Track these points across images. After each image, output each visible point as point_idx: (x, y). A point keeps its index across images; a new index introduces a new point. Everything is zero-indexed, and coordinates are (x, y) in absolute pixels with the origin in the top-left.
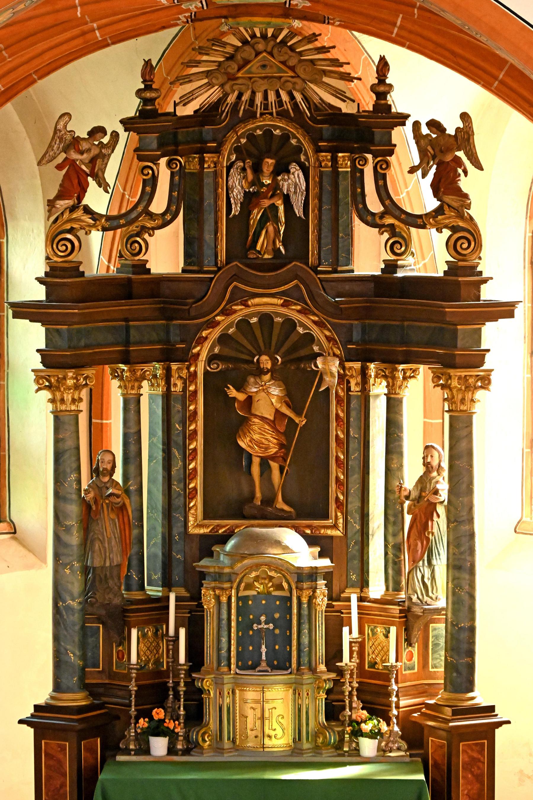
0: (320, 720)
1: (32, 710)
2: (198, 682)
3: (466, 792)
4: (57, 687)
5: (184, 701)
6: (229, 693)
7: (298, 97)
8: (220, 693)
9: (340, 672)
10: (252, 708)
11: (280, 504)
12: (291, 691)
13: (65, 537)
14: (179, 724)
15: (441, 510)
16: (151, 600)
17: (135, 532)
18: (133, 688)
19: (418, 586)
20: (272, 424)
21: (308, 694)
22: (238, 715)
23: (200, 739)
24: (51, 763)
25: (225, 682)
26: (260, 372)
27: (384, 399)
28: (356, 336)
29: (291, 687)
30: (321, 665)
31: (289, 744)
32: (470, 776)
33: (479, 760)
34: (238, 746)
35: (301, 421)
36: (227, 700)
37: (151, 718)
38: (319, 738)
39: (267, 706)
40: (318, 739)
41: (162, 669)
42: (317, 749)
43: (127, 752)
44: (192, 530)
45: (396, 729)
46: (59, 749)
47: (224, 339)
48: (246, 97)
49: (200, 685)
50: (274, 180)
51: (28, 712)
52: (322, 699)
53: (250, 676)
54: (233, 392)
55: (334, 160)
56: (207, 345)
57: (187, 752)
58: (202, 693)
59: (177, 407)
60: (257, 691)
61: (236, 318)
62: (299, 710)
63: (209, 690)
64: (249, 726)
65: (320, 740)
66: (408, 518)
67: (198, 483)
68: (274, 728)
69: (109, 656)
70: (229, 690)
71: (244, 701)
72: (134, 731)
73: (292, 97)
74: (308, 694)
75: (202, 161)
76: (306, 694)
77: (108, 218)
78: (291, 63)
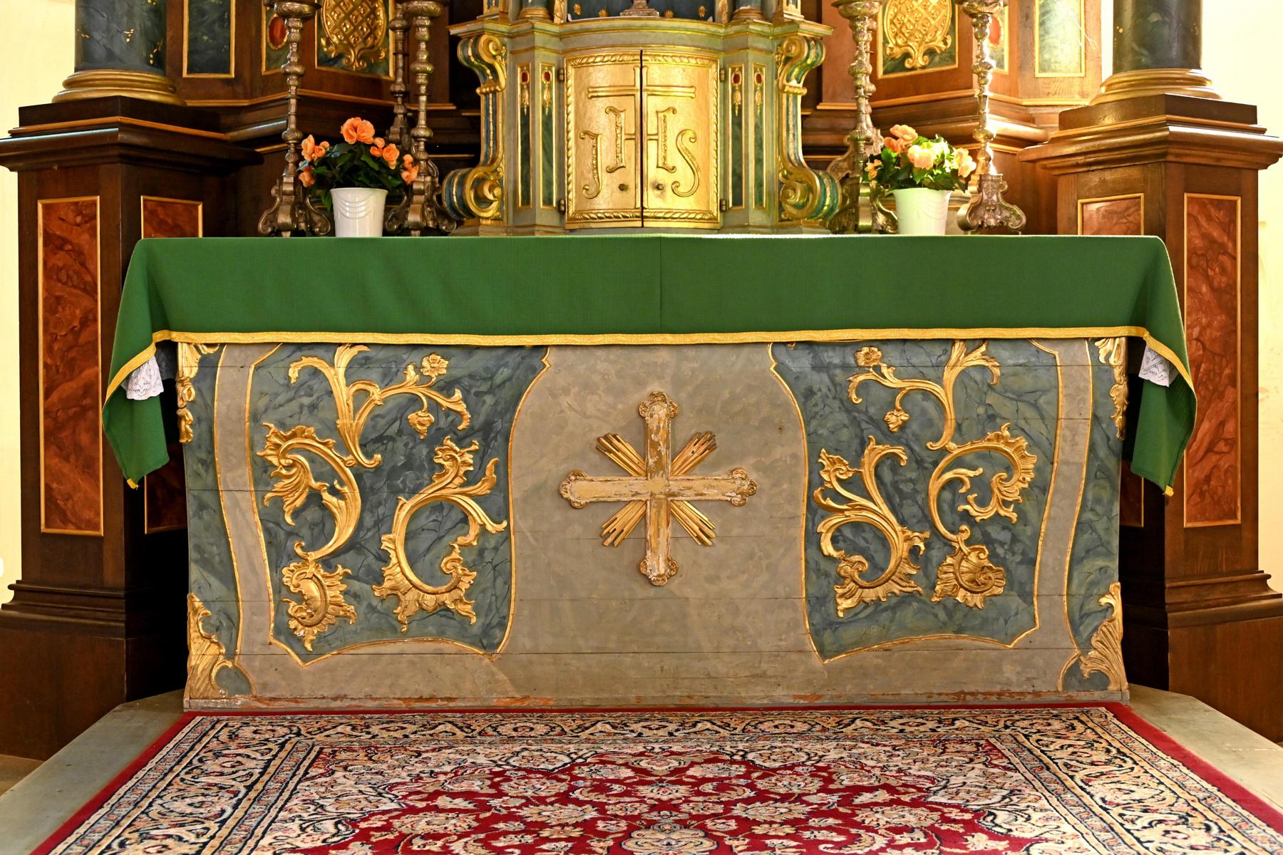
0: (791, 152)
1: (14, 123)
2: (465, 46)
3: (1196, 331)
4: (86, 57)
5: (429, 101)
6: (547, 77)
8: (524, 78)
10: (612, 110)
12: (714, 71)
14: (416, 161)
21: (759, 79)
22: (572, 135)
23: (470, 196)
24: (60, 259)
25: (539, 39)
29: (715, 61)
30: (792, 6)
31: (711, 213)
32: (1204, 289)
33: (1225, 253)
34: (573, 220)
36: (544, 95)
37: (337, 140)
38: (794, 190)
39: (652, 104)
40: (791, 193)
41: (386, 78)
45: (993, 171)
46: (79, 219)
49: (470, 53)
52: (795, 95)
58: (479, 85)
60: (622, 62)
62: (737, 123)
63: (494, 72)
64: (605, 160)
65: (795, 198)
68: (670, 164)
70: (550, 68)
72: (291, 180)
74: (759, 79)
76: (753, 77)
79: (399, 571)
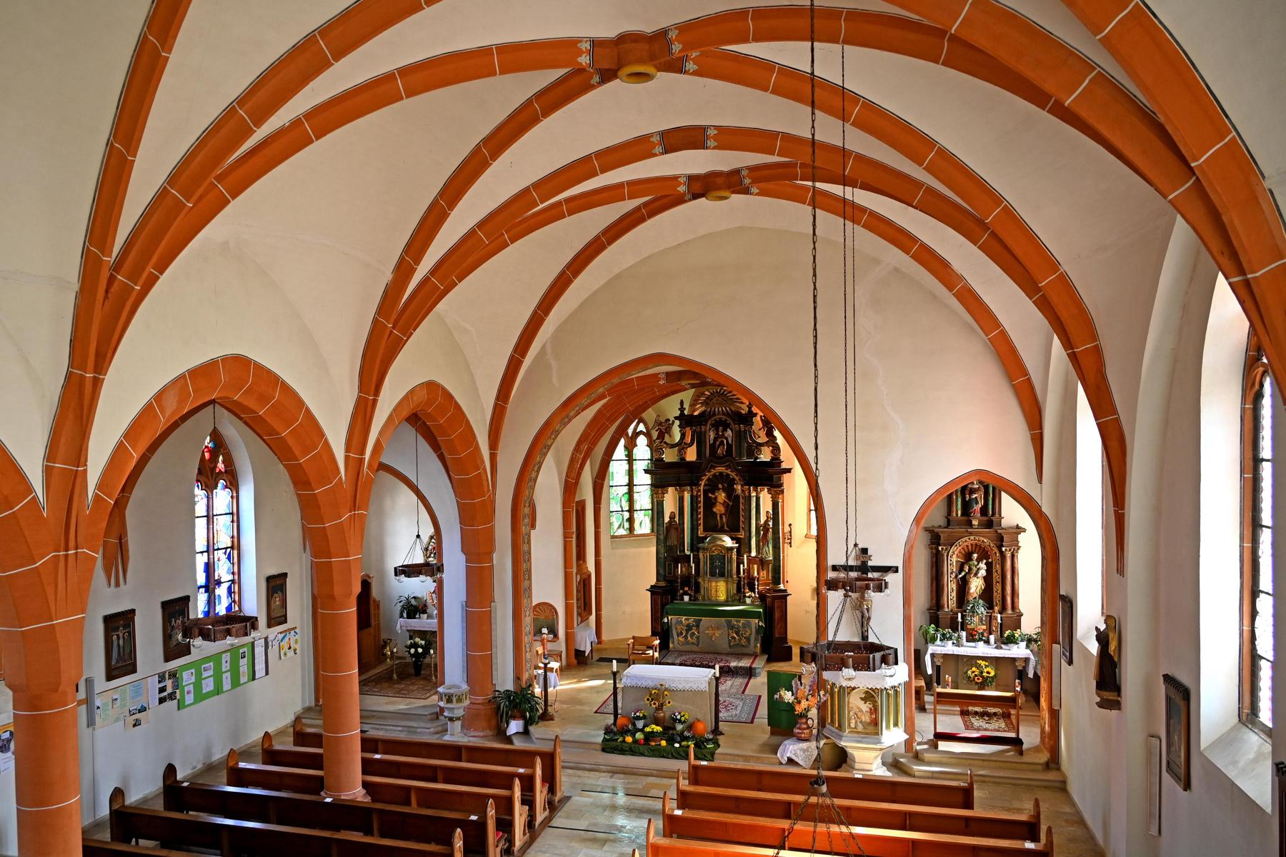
4: (657, 580)
7: (728, 409)
9: (740, 578)
11: (726, 528)
13: (660, 537)
15: (771, 530)
16: (686, 555)
17: (682, 536)
18: (679, 581)
19: (765, 553)
20: (723, 504)
26: (719, 489)
27: (755, 498)
28: (747, 478)
35: (731, 504)
42: (733, 601)
43: (677, 600)
44: (700, 535)
45: (757, 596)
47: (709, 479)
48: (713, 409)
50: (723, 433)
51: (648, 588)
53: (713, 579)
54: (710, 495)
55: (740, 427)
56: (704, 481)
57: (694, 601)
59: (695, 499)
61: (712, 473)
66: (762, 532)
67: (701, 521)
69: (674, 572)
71: (711, 586)
73: (726, 409)
75: (701, 428)
77: (672, 445)
78: (725, 399)
79: (689, 638)
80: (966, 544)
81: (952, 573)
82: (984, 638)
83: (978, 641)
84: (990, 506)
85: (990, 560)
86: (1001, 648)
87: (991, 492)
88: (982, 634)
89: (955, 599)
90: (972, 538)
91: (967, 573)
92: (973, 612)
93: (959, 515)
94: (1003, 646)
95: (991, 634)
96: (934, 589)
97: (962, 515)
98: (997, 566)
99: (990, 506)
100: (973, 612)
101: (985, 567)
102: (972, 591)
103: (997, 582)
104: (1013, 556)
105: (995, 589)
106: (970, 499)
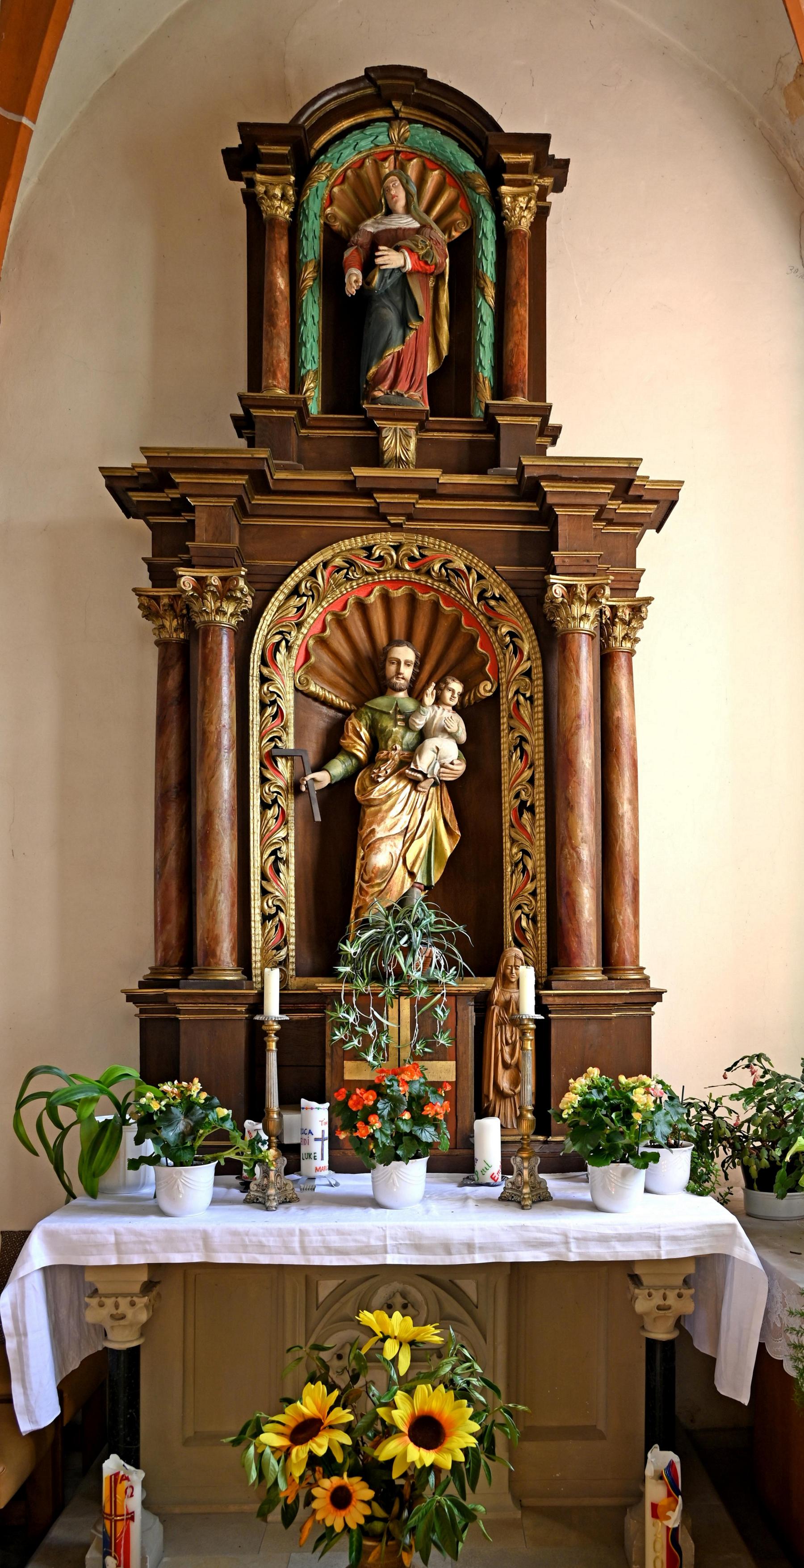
80: (350, 591)
81: (269, 759)
82: (427, 1135)
83: (390, 1157)
84: (486, 357)
85: (486, 689)
86: (542, 1198)
87: (488, 268)
88: (417, 1103)
89: (289, 918)
90: (383, 542)
91: (360, 766)
92: (379, 977)
93: (314, 408)
94: (554, 1184)
95: (482, 1112)
96: (172, 862)
97: (326, 408)
98: (525, 712)
99: (486, 357)
100: (379, 977)
101: (458, 725)
102: (381, 859)
103: (523, 807)
104: (604, 631)
105: (511, 852)
106: (364, 292)
